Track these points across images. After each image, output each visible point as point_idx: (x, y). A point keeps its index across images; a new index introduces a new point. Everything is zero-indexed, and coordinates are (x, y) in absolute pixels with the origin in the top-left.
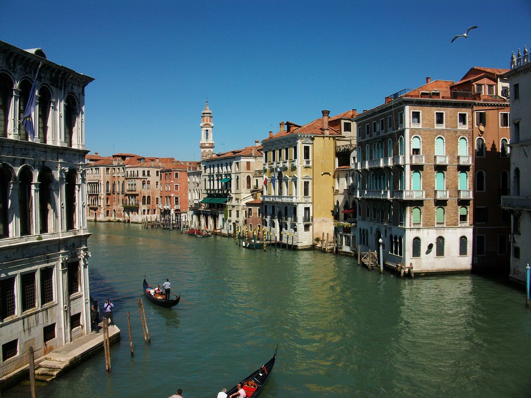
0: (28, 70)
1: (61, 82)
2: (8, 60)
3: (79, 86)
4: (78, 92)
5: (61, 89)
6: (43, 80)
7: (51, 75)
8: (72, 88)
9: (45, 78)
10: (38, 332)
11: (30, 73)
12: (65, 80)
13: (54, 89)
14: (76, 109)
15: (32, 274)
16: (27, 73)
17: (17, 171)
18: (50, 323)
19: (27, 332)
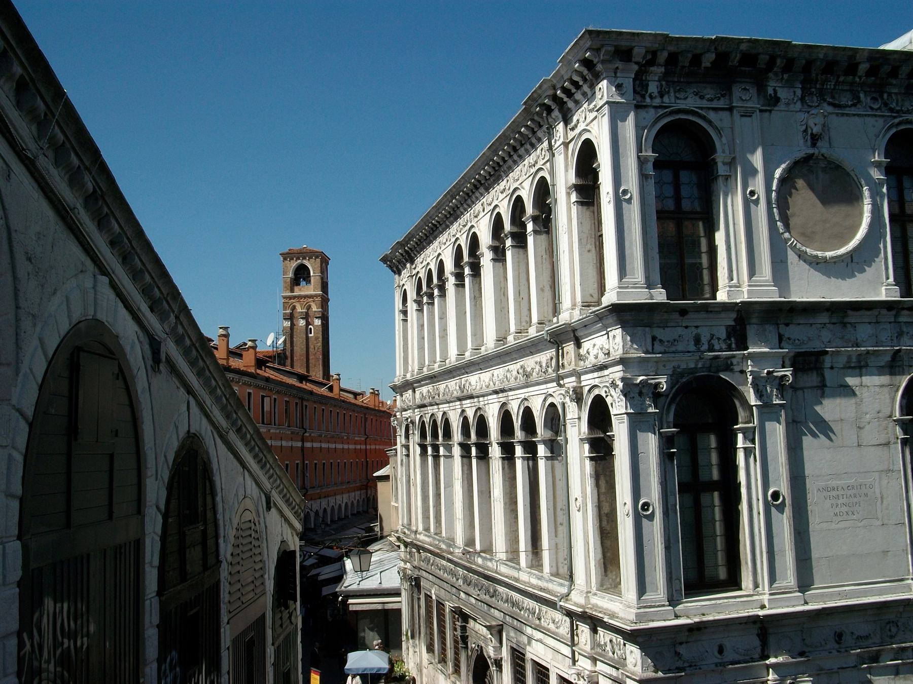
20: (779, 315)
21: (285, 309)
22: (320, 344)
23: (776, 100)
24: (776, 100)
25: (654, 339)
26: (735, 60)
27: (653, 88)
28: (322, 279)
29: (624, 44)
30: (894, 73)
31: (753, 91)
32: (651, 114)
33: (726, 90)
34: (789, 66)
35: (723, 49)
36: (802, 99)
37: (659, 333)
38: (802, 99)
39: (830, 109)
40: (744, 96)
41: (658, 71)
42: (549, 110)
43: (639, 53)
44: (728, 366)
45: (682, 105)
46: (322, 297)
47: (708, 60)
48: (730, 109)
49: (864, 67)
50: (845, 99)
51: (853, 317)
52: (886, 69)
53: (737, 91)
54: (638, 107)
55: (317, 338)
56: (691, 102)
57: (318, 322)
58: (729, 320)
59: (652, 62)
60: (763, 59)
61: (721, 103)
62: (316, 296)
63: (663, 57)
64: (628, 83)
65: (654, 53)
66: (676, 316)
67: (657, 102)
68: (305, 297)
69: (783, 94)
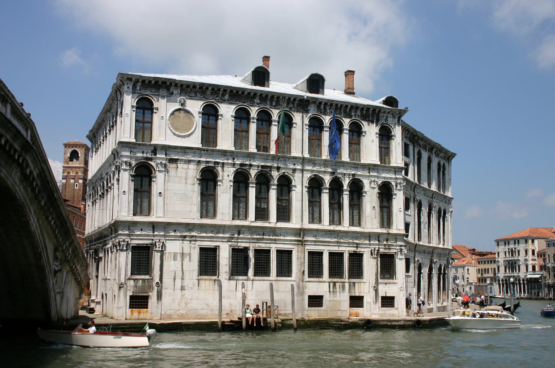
0: (338, 112)
1: (373, 116)
2: (319, 107)
3: (394, 117)
4: (394, 122)
5: (372, 122)
6: (354, 118)
7: (362, 112)
8: (386, 120)
9: (355, 116)
10: (344, 298)
11: (340, 113)
12: (378, 114)
13: (365, 123)
14: (392, 136)
15: (341, 255)
16: (337, 114)
17: (327, 179)
18: (357, 295)
19: (332, 293)
20: (166, 149)
21: (64, 173)
22: (81, 193)
23: (172, 94)
24: (172, 94)
25: (131, 151)
26: (160, 83)
27: (138, 88)
28: (85, 159)
29: (130, 77)
30: (207, 88)
31: (166, 91)
32: (137, 95)
33: (158, 90)
34: (176, 85)
35: (157, 80)
36: (180, 94)
37: (133, 150)
38: (180, 94)
39: (188, 97)
40: (163, 92)
41: (139, 84)
42: (117, 92)
43: (134, 79)
44: (151, 159)
45: (145, 93)
46: (84, 168)
47: (153, 82)
48: (159, 95)
49: (198, 87)
50: (193, 95)
51: (187, 151)
52: (204, 88)
53: (161, 91)
54: (133, 93)
55: (79, 190)
56: (148, 92)
57: (81, 181)
58: (152, 148)
59: (138, 81)
60: (168, 83)
61: (157, 94)
62: (82, 167)
63: (140, 80)
64: (131, 87)
65: (138, 80)
66: (138, 146)
67: (139, 92)
68: (75, 167)
69: (175, 92)
